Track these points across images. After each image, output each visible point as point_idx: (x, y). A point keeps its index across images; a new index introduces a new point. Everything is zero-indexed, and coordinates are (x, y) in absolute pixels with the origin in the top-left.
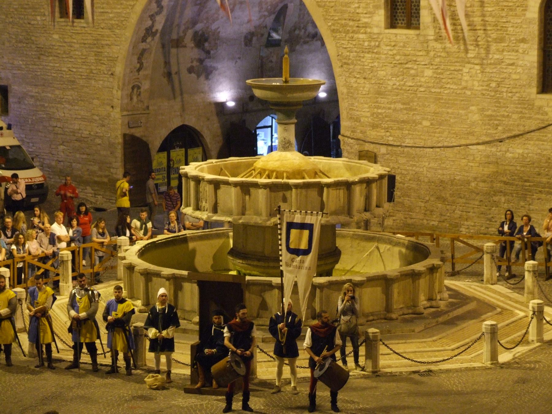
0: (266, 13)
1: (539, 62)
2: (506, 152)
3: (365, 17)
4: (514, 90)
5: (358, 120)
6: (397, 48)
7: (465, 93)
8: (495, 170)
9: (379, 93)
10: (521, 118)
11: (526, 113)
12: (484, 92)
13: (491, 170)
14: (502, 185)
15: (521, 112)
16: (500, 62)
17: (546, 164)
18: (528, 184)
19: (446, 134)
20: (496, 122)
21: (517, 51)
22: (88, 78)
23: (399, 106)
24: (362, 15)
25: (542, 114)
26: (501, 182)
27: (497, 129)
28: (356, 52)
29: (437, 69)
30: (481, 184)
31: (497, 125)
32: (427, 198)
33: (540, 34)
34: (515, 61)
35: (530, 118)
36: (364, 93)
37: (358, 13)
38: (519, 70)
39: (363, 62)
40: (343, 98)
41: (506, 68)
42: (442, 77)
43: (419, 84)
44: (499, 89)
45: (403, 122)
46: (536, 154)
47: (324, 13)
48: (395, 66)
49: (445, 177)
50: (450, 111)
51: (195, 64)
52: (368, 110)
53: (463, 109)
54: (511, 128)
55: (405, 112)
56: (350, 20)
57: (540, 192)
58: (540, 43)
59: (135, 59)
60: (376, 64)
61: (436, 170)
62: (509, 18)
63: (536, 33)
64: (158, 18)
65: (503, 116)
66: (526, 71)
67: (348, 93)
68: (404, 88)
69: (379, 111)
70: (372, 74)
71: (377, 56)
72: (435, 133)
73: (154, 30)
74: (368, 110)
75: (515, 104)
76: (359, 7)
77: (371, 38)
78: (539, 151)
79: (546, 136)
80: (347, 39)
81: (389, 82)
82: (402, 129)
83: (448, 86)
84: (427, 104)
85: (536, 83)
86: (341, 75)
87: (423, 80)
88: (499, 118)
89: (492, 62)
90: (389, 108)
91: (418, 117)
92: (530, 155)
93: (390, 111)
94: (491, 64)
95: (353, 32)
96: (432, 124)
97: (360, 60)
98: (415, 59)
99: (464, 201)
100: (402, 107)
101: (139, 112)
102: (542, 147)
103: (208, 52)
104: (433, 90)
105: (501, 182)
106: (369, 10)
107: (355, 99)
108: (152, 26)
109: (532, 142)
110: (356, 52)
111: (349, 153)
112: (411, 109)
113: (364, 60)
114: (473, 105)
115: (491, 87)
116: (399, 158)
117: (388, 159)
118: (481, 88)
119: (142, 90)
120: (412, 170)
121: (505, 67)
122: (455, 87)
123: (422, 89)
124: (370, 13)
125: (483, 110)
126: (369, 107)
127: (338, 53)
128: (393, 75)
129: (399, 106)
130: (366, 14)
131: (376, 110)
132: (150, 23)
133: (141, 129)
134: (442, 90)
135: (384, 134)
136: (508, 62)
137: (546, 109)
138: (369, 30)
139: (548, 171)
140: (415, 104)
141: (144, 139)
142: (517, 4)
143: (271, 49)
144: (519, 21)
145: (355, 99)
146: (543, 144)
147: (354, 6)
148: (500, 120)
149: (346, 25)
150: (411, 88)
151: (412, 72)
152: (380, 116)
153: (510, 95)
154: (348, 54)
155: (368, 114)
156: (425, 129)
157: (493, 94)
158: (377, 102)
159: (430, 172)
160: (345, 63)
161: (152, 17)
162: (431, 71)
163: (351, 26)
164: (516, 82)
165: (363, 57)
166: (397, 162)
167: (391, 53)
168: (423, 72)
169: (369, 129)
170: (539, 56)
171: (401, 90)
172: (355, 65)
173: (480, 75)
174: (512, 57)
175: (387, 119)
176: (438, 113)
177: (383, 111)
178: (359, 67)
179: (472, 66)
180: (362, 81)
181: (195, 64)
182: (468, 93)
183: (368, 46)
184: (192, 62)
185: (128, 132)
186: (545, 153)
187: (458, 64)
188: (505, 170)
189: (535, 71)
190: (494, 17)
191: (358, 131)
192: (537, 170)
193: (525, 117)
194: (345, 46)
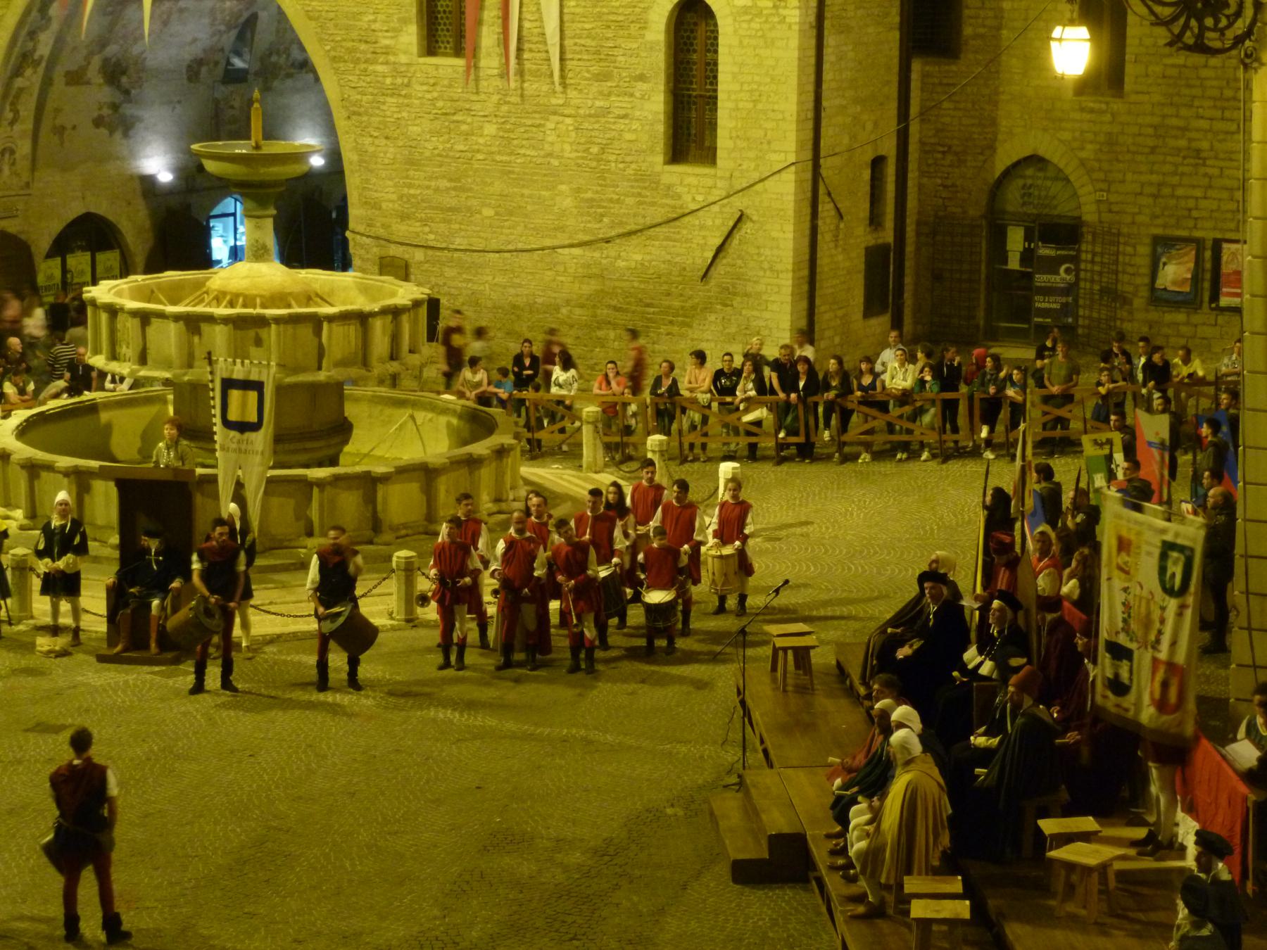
0: (223, 28)
2: (616, 259)
3: (385, 37)
4: (628, 159)
5: (376, 206)
6: (438, 88)
8: (598, 288)
10: (640, 203)
11: (647, 196)
12: (580, 161)
13: (594, 288)
14: (610, 312)
15: (639, 194)
16: (606, 112)
17: (680, 279)
18: (652, 310)
19: (520, 229)
20: (599, 210)
21: (632, 95)
23: (444, 184)
24: (380, 34)
25: (672, 197)
26: (609, 306)
27: (601, 221)
28: (372, 94)
29: (503, 123)
30: (578, 311)
31: (602, 215)
33: (667, 68)
34: (629, 111)
35: (653, 204)
36: (386, 161)
37: (374, 31)
39: (384, 111)
40: (352, 171)
41: (615, 123)
42: (512, 136)
43: (476, 147)
44: (604, 157)
45: (451, 209)
46: (664, 262)
47: (319, 30)
48: (436, 118)
50: (526, 192)
52: (392, 190)
53: (547, 189)
54: (624, 220)
55: (453, 193)
56: (360, 41)
57: (671, 322)
58: (667, 83)
60: (405, 114)
61: (505, 287)
62: (620, 41)
63: (662, 65)
65: (611, 200)
66: (647, 128)
67: (361, 161)
68: (451, 154)
69: (412, 191)
70: (398, 131)
71: (406, 101)
72: (502, 227)
73: (36, 56)
74: (392, 190)
75: (629, 180)
76: (375, 21)
77: (396, 71)
78: (668, 257)
79: (679, 233)
80: (358, 72)
81: (426, 145)
82: (449, 222)
83: (522, 151)
84: (488, 180)
86: (347, 133)
87: (481, 141)
88: (605, 204)
89: (593, 112)
90: (428, 187)
93: (430, 192)
94: (590, 116)
95: (366, 62)
96: (497, 214)
97: (378, 108)
98: (468, 106)
100: (448, 185)
101: (13, 193)
103: (127, 92)
104: (498, 158)
105: (609, 306)
106: (392, 25)
107: (371, 171)
109: (657, 243)
110: (372, 94)
111: (363, 260)
112: (463, 189)
113: (385, 108)
114: (562, 183)
115: (591, 154)
116: (447, 269)
117: (426, 271)
118: (574, 155)
119: (17, 156)
120: (466, 288)
121: (612, 120)
122: (533, 153)
123: (480, 156)
124: (394, 30)
125: (578, 190)
126: (395, 186)
127: (342, 94)
128: (430, 132)
129: (444, 184)
130: (387, 31)
131: (406, 190)
134: (513, 158)
135: (419, 229)
136: (617, 112)
137: (679, 189)
138: (392, 58)
140: (469, 180)
141: (23, 237)
142: (631, 18)
143: (231, 88)
144: (635, 46)
145: (371, 171)
146: (674, 246)
147: (367, 19)
148: (604, 207)
150: (463, 154)
151: (464, 127)
152: (413, 200)
153: (621, 166)
154: (359, 97)
155: (394, 197)
156: (487, 222)
157: (594, 164)
158: (407, 177)
159: (495, 291)
160: (354, 113)
162: (495, 126)
163: (363, 52)
165: (384, 103)
167: (428, 96)
168: (481, 128)
169: (395, 221)
170: (666, 103)
171: (447, 156)
172: (371, 116)
173: (573, 134)
174: (624, 105)
175: (425, 205)
176: (507, 196)
177: (418, 192)
179: (561, 118)
180: (384, 142)
181: (106, 111)
182: (555, 162)
183: (392, 84)
184: (100, 109)
186: (678, 259)
187: (534, 115)
188: (615, 288)
189: (660, 128)
190: (594, 39)
191: (378, 224)
192: (665, 287)
194: (353, 85)
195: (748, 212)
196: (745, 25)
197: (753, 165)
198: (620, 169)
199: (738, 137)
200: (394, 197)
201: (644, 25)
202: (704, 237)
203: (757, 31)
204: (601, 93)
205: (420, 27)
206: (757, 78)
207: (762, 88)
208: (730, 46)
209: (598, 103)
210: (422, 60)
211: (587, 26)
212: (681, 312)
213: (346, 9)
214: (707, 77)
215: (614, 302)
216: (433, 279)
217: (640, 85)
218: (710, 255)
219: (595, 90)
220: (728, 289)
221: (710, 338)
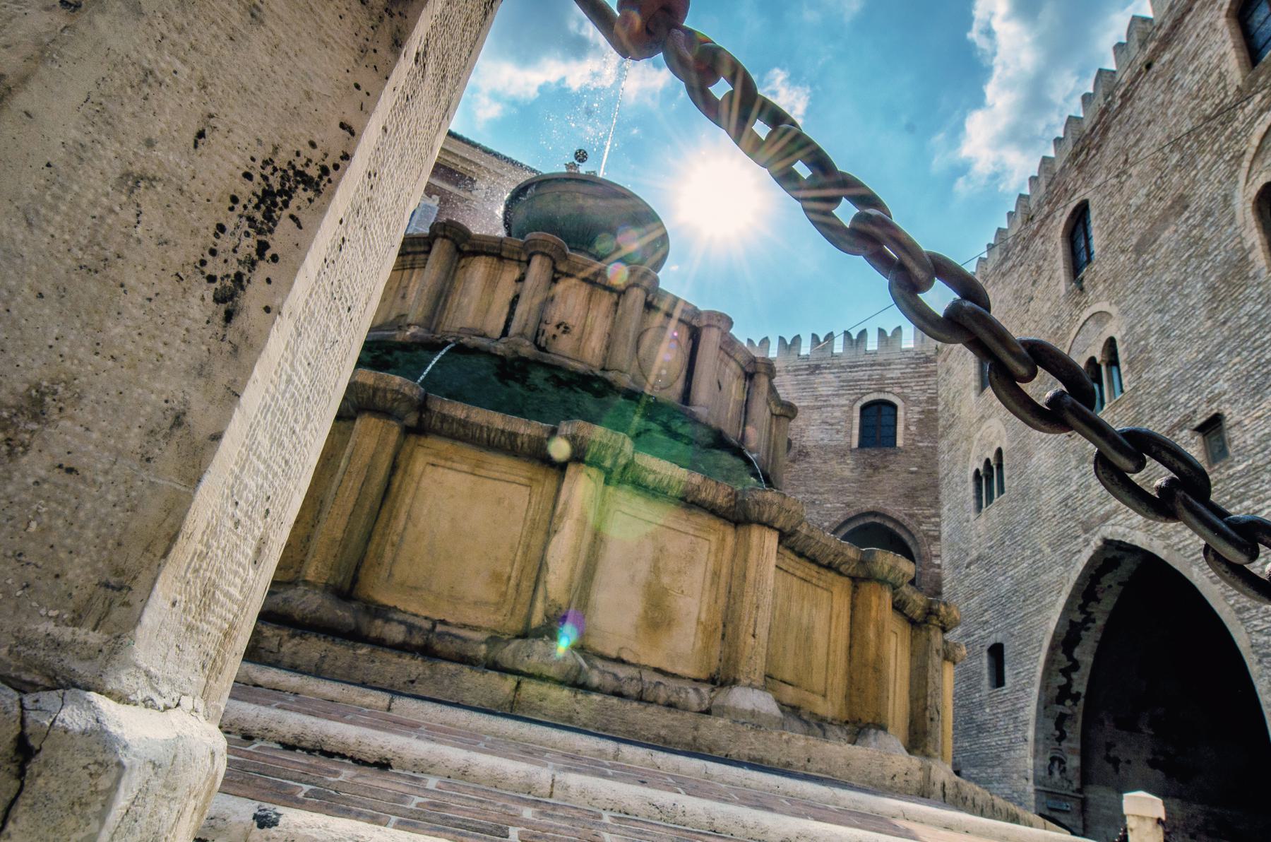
22: (1010, 749)
47: (1223, 590)
59: (1051, 724)
64: (1074, 676)
80: (1260, 615)
86: (1261, 676)
119: (1067, 766)
133: (1069, 817)
161: (1066, 672)
194: (1258, 628)
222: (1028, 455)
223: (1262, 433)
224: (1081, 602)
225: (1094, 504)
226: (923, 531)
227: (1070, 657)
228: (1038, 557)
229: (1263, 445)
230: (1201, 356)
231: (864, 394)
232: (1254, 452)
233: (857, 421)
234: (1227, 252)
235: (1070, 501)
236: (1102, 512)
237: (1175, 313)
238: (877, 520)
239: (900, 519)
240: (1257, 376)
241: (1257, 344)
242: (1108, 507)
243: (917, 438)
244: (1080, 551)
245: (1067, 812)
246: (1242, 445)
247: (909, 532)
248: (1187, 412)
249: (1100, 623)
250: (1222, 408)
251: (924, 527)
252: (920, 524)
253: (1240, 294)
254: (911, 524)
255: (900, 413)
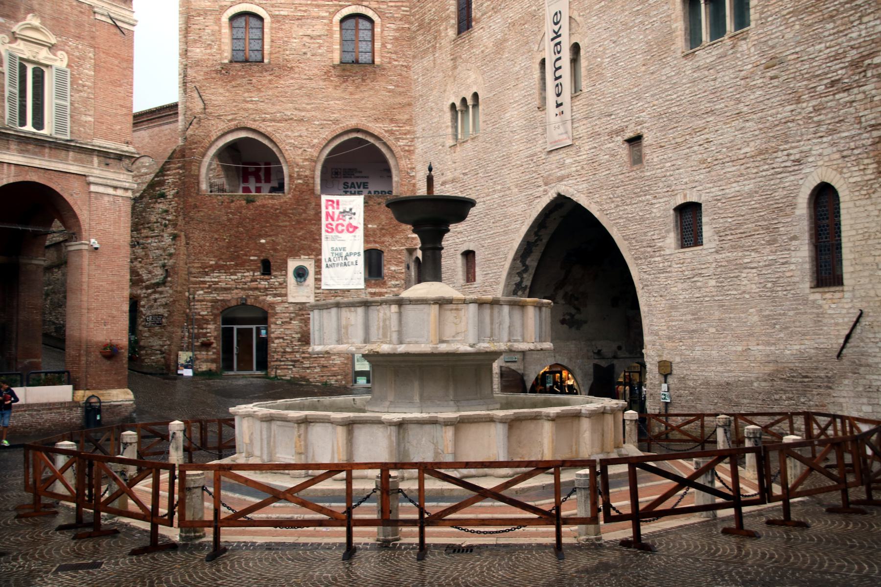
1: (809, 256)
4: (788, 288)
6: (685, 265)
7: (744, 297)
8: (775, 368)
9: (672, 307)
10: (797, 314)
17: (824, 358)
18: (806, 380)
23: (689, 317)
28: (654, 274)
29: (719, 278)
30: (763, 384)
31: (775, 324)
32: (716, 401)
33: (811, 229)
36: (661, 309)
38: (793, 267)
41: (779, 268)
44: (775, 289)
45: (693, 331)
48: (685, 282)
49: (730, 379)
50: (732, 315)
51: (567, 317)
53: (743, 312)
58: (811, 238)
60: (669, 282)
61: (722, 372)
63: (806, 228)
64: (525, 276)
65: (780, 314)
66: (799, 267)
67: (649, 310)
69: (673, 324)
72: (719, 338)
75: (790, 301)
76: (654, 235)
78: (816, 345)
79: (821, 330)
81: (681, 297)
82: (692, 338)
83: (729, 293)
85: (808, 277)
86: (642, 296)
87: (707, 290)
89: (767, 263)
90: (681, 320)
91: (705, 325)
92: (807, 350)
93: (682, 323)
94: (766, 266)
96: (717, 330)
98: (700, 272)
99: (748, 401)
100: (691, 317)
102: (818, 341)
104: (717, 298)
107: (654, 315)
108: (521, 282)
110: (654, 274)
111: (650, 364)
112: (699, 319)
116: (692, 365)
120: (702, 375)
122: (735, 292)
123: (707, 299)
127: (640, 276)
128: (683, 290)
129: (689, 317)
132: (518, 279)
133: (516, 364)
137: (820, 302)
138: (662, 253)
139: (827, 365)
140: (702, 313)
141: (519, 372)
142: (787, 204)
144: (789, 220)
145: (654, 315)
146: (819, 338)
147: (650, 234)
149: (645, 252)
150: (698, 299)
151: (699, 284)
153: (785, 293)
155: (665, 328)
156: (712, 335)
157: (769, 294)
161: (520, 274)
164: (789, 279)
165: (659, 278)
166: (689, 369)
167: (680, 270)
168: (706, 283)
169: (665, 341)
170: (810, 251)
171: (690, 302)
173: (756, 278)
177: (677, 323)
178: (656, 287)
179: (750, 270)
181: (567, 317)
182: (747, 296)
185: (504, 365)
186: (822, 346)
189: (807, 266)
190: (765, 221)
192: (815, 364)
193: (800, 313)
195: (865, 310)
196: (857, 193)
197: (867, 280)
198: (784, 295)
199: (856, 264)
200: (665, 328)
201: (793, 206)
202: (838, 331)
203: (865, 195)
204: (771, 251)
205: (678, 235)
206: (867, 225)
207: (870, 230)
208: (848, 208)
209: (770, 258)
210: (677, 251)
211: (763, 214)
212: (826, 380)
213: (641, 231)
214: (837, 233)
215: (785, 377)
216: (685, 372)
217: (794, 243)
218: (842, 341)
219: (768, 250)
220: (854, 362)
221: (845, 395)
222: (502, 109)
223: (662, 157)
224: (536, 230)
225: (553, 167)
226: (400, 146)
227: (524, 264)
228: (507, 192)
229: (662, 165)
230: (635, 90)
231: (343, 7)
232: (657, 167)
233: (337, 36)
234: (662, 23)
235: (535, 158)
236: (559, 174)
237: (623, 49)
238: (360, 136)
239: (380, 136)
240: (665, 120)
241: (669, 98)
242: (563, 172)
243: (394, 56)
244: (540, 197)
245: (515, 362)
246: (651, 160)
247: (388, 148)
248: (622, 124)
249: (545, 241)
250: (643, 131)
251: (401, 143)
252: (397, 139)
253: (665, 58)
254: (391, 141)
255: (377, 30)
